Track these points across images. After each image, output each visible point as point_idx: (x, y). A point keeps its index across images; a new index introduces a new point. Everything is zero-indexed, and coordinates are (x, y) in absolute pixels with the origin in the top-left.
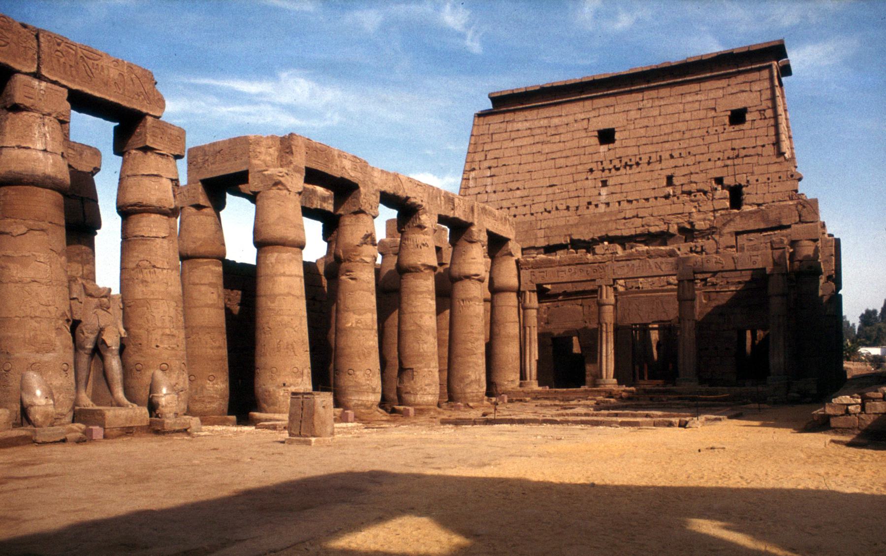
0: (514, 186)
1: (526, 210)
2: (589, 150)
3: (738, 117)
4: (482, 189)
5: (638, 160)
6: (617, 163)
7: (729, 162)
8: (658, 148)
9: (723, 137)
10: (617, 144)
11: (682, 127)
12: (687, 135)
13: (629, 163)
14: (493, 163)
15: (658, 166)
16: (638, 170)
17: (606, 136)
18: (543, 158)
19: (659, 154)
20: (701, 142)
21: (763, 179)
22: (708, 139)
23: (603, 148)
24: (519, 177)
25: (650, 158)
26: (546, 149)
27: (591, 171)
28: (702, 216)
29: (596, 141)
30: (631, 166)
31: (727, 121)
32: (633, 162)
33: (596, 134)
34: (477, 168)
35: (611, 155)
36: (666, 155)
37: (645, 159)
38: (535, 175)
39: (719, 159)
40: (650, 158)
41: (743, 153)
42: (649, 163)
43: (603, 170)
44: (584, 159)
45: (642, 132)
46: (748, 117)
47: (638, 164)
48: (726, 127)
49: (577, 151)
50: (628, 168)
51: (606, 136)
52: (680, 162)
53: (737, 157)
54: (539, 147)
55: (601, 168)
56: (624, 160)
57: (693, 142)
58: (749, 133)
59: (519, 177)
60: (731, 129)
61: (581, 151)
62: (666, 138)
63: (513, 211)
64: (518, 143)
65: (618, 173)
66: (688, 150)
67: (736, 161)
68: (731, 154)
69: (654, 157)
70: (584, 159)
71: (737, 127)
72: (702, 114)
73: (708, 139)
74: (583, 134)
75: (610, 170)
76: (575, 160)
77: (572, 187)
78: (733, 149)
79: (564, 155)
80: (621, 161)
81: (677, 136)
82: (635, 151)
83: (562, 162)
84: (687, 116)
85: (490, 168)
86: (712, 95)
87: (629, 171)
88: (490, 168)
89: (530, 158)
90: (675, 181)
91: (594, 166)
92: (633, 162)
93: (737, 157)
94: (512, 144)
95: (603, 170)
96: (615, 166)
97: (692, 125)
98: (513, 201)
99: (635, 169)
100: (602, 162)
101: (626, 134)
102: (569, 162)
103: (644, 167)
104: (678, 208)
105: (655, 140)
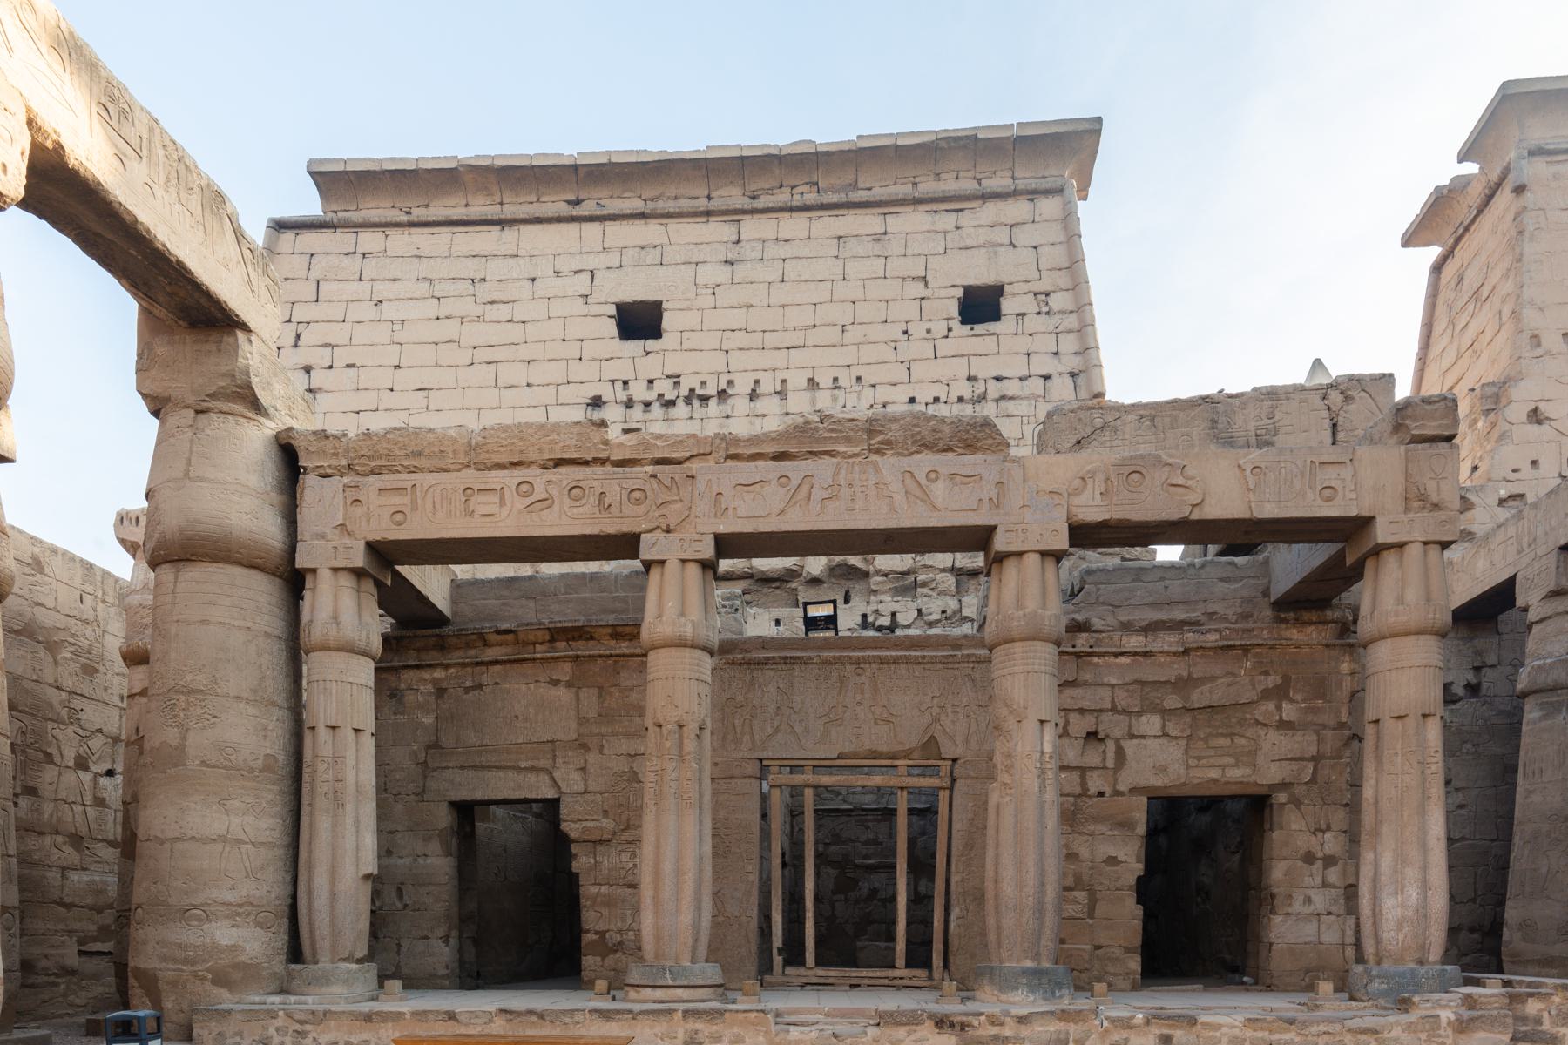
2: (589, 349)
3: (980, 306)
5: (723, 386)
6: (665, 387)
8: (779, 359)
9: (945, 347)
10: (668, 340)
11: (841, 314)
12: (849, 337)
13: (699, 392)
14: (320, 358)
16: (726, 409)
17: (638, 322)
19: (780, 376)
20: (891, 356)
22: (908, 350)
23: (635, 346)
25: (757, 382)
26: (475, 333)
27: (597, 402)
29: (611, 328)
30: (704, 399)
31: (954, 309)
32: (711, 390)
33: (613, 311)
36: (797, 380)
37: (743, 386)
38: (436, 399)
39: (936, 400)
40: (757, 382)
42: (753, 396)
43: (629, 404)
44: (579, 371)
45: (737, 318)
46: (1008, 305)
47: (722, 395)
48: (951, 323)
49: (558, 350)
50: (696, 403)
51: (638, 322)
53: (983, 398)
54: (450, 329)
55: (622, 396)
57: (869, 353)
58: (1008, 343)
60: (961, 330)
61: (573, 350)
65: (673, 412)
66: (855, 372)
69: (766, 387)
70: (579, 371)
71: (979, 328)
72: (890, 289)
73: (908, 350)
75: (647, 404)
78: (971, 379)
79: (524, 352)
80: (677, 384)
81: (833, 334)
82: (718, 362)
86: (915, 248)
89: (428, 354)
91: (606, 392)
92: (711, 390)
93: (983, 398)
95: (629, 404)
96: (661, 396)
97: (864, 312)
100: (625, 383)
101: (691, 319)
102: (537, 374)
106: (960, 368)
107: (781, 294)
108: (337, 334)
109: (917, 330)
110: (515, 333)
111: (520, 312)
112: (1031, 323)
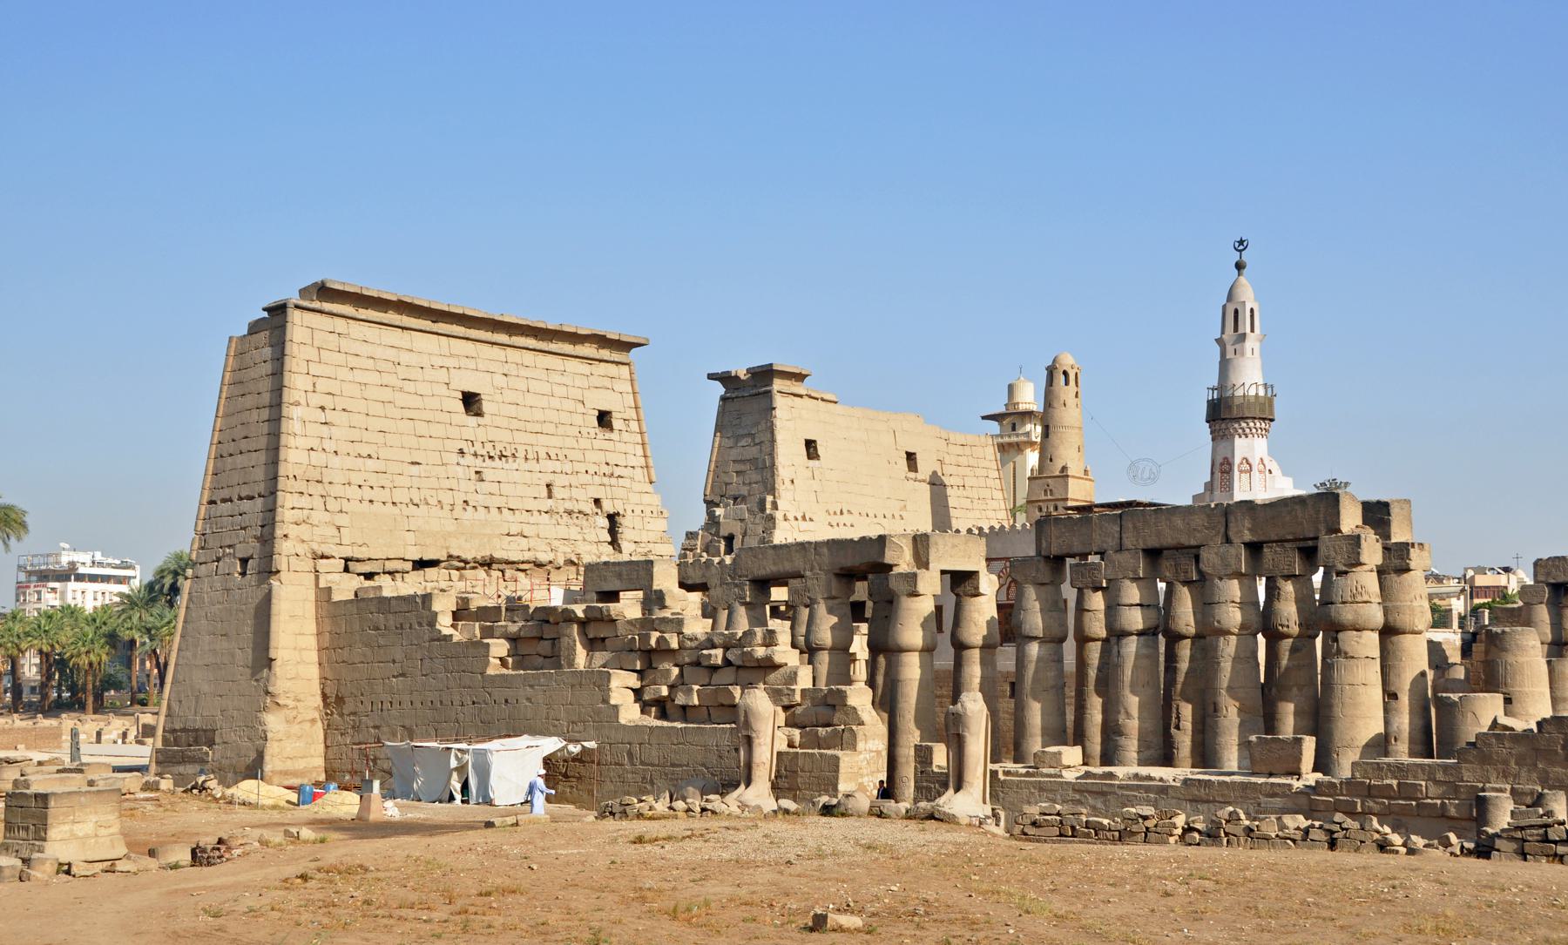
0: (365, 451)
1: (385, 495)
4: (315, 443)
7: (606, 480)
8: (531, 438)
9: (598, 444)
14: (328, 402)
15: (532, 465)
16: (515, 466)
18: (397, 413)
21: (638, 512)
22: (584, 443)
24: (366, 436)
28: (588, 547)
29: (460, 406)
34: (303, 402)
35: (481, 435)
37: (521, 454)
41: (618, 471)
52: (557, 466)
54: (387, 394)
56: (499, 447)
59: (366, 436)
62: (538, 428)
63: (367, 493)
64: (359, 376)
67: (613, 481)
68: (607, 470)
74: (443, 390)
76: (437, 430)
77: (441, 471)
79: (428, 415)
83: (422, 428)
84: (555, 402)
85: (323, 408)
87: (506, 466)
88: (323, 408)
90: (555, 490)
94: (349, 376)
98: (367, 475)
99: (511, 464)
103: (520, 460)
104: (562, 531)
105: (530, 427)
106: (600, 457)
107: (530, 400)
108: (333, 386)
109: (584, 431)
110: (418, 402)
111: (423, 388)
112: (625, 436)
